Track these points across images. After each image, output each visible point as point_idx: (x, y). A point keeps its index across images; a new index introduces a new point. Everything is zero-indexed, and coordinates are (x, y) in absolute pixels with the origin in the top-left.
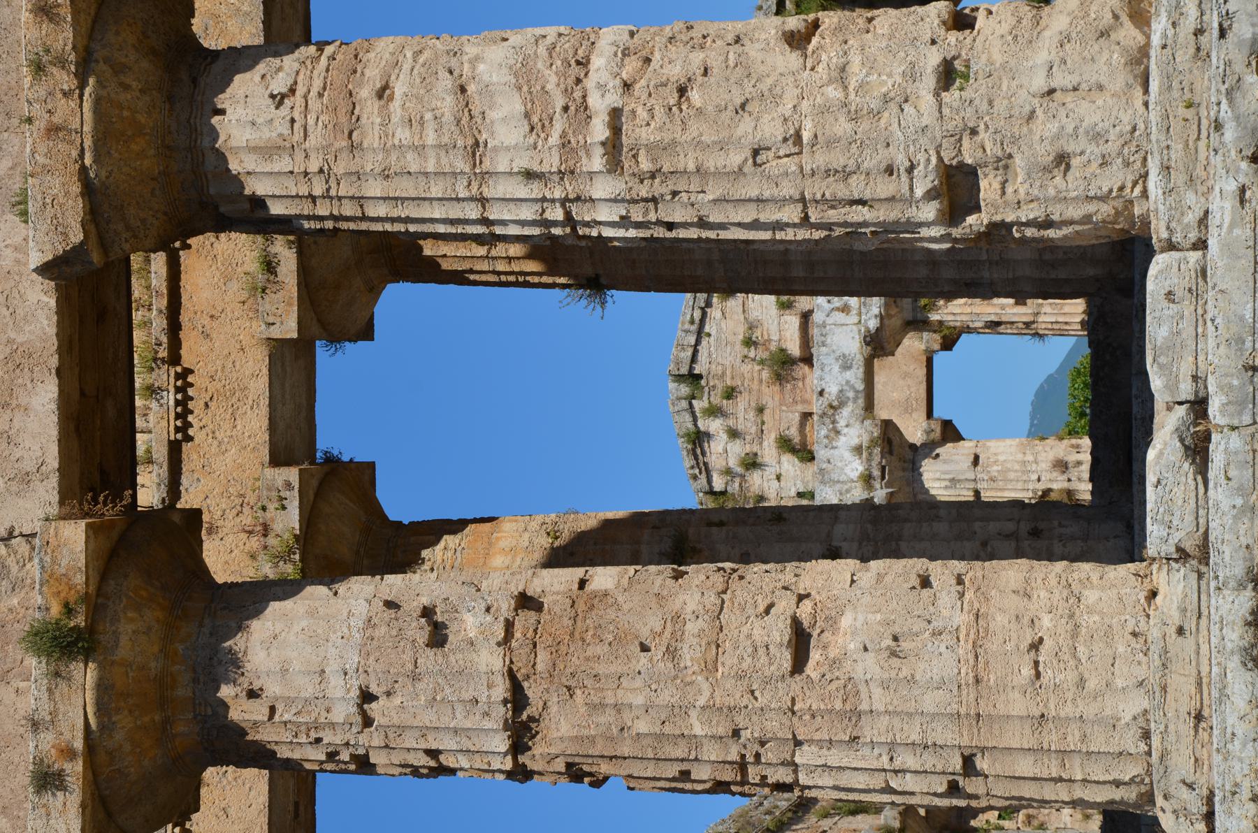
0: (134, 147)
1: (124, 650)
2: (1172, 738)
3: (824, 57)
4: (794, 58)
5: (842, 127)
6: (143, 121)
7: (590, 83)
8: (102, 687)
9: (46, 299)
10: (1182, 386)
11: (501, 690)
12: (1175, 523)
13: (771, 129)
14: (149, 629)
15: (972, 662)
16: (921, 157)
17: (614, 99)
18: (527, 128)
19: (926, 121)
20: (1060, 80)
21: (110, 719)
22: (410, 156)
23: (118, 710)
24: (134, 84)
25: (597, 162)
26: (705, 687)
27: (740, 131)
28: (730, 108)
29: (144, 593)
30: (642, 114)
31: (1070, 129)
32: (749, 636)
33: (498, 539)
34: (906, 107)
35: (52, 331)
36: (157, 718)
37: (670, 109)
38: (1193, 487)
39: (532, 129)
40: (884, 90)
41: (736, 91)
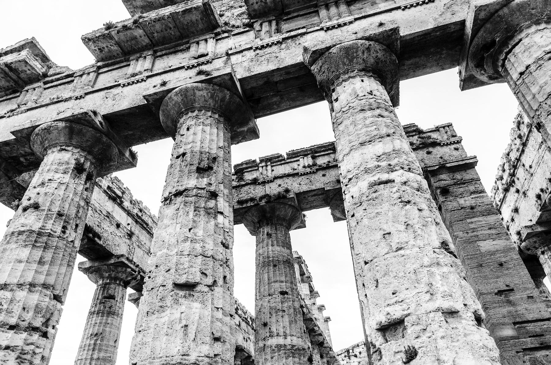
0: (345, 60)
1: (198, 93)
3: (441, 256)
4: (437, 244)
7: (402, 171)
8: (187, 90)
11: (181, 189)
14: (207, 101)
18: (379, 155)
19: (424, 305)
23: (181, 95)
28: (407, 220)
29: (217, 99)
30: (394, 190)
32: (192, 266)
34: (429, 295)
41: (415, 221)
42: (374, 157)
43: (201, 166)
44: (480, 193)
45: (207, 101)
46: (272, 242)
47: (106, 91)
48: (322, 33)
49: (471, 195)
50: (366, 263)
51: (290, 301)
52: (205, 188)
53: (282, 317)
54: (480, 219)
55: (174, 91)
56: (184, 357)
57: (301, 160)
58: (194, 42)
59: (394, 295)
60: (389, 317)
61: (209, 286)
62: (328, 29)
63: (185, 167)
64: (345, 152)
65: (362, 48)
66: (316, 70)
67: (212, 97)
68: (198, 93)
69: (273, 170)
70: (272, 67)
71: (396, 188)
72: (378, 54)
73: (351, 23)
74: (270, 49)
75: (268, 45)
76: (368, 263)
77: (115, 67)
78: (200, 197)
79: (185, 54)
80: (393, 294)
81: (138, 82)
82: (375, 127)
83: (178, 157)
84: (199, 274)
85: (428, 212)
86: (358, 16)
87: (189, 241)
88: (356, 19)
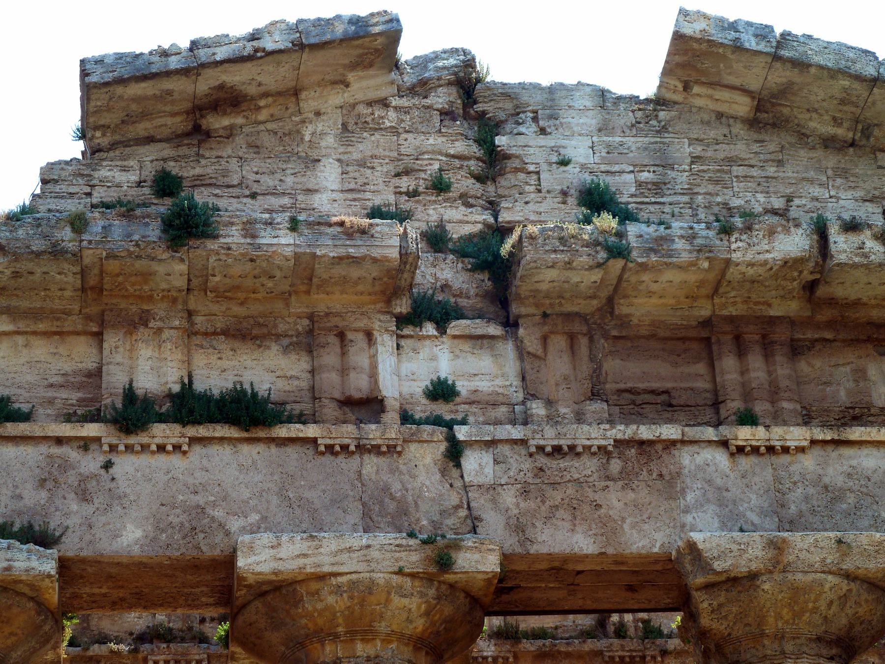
0: (785, 611)
1: (397, 601)
6: (804, 618)
8: (371, 587)
9: (658, 545)
21: (345, 592)
23: (351, 598)
24: (831, 612)
35: (634, 549)
36: (340, 629)
45: (411, 622)
47: (43, 448)
48: (721, 458)
55: (334, 581)
58: (330, 330)
62: (740, 450)
65: (831, 596)
66: (705, 605)
67: (427, 613)
68: (397, 601)
70: (582, 542)
72: (860, 610)
73: (801, 450)
74: (576, 463)
75: (572, 448)
77: (41, 327)
79: (294, 357)
81: (161, 448)
86: (821, 437)
88: (813, 442)
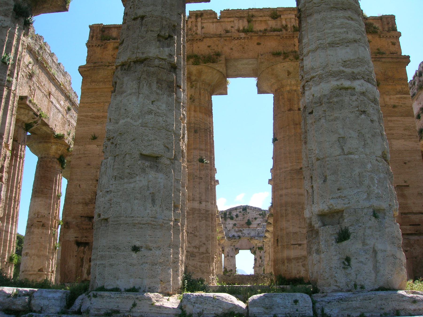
2: (108, 300)
3: (381, 164)
4: (379, 153)
5: (357, 171)
7: (362, 81)
10: (255, 308)
12: (196, 305)
13: (353, 143)
15: (142, 222)
16: (346, 201)
17: (358, 89)
18: (345, 60)
20: (380, 256)
22: (330, 25)
25: (334, 83)
26: (138, 123)
27: (351, 131)
30: (354, 98)
31: (362, 259)
32: (156, 139)
33: (207, 116)
37: (357, 107)
38: (211, 312)
39: (345, 62)
40: (372, 186)
42: (340, 61)
43: (162, 33)
44: (404, 94)
46: (195, 107)
49: (396, 94)
50: (318, 159)
51: (207, 169)
52: (166, 59)
53: (199, 183)
54: (399, 118)
56: (153, 219)
57: (235, 22)
59: (339, 191)
60: (331, 207)
61: (170, 159)
63: (145, 33)
64: (310, 48)
69: (203, 28)
71: (356, 96)
76: (319, 160)
78: (162, 68)
80: (338, 189)
82: (345, 30)
83: (135, 19)
84: (162, 147)
85: (377, 124)
87: (153, 114)
